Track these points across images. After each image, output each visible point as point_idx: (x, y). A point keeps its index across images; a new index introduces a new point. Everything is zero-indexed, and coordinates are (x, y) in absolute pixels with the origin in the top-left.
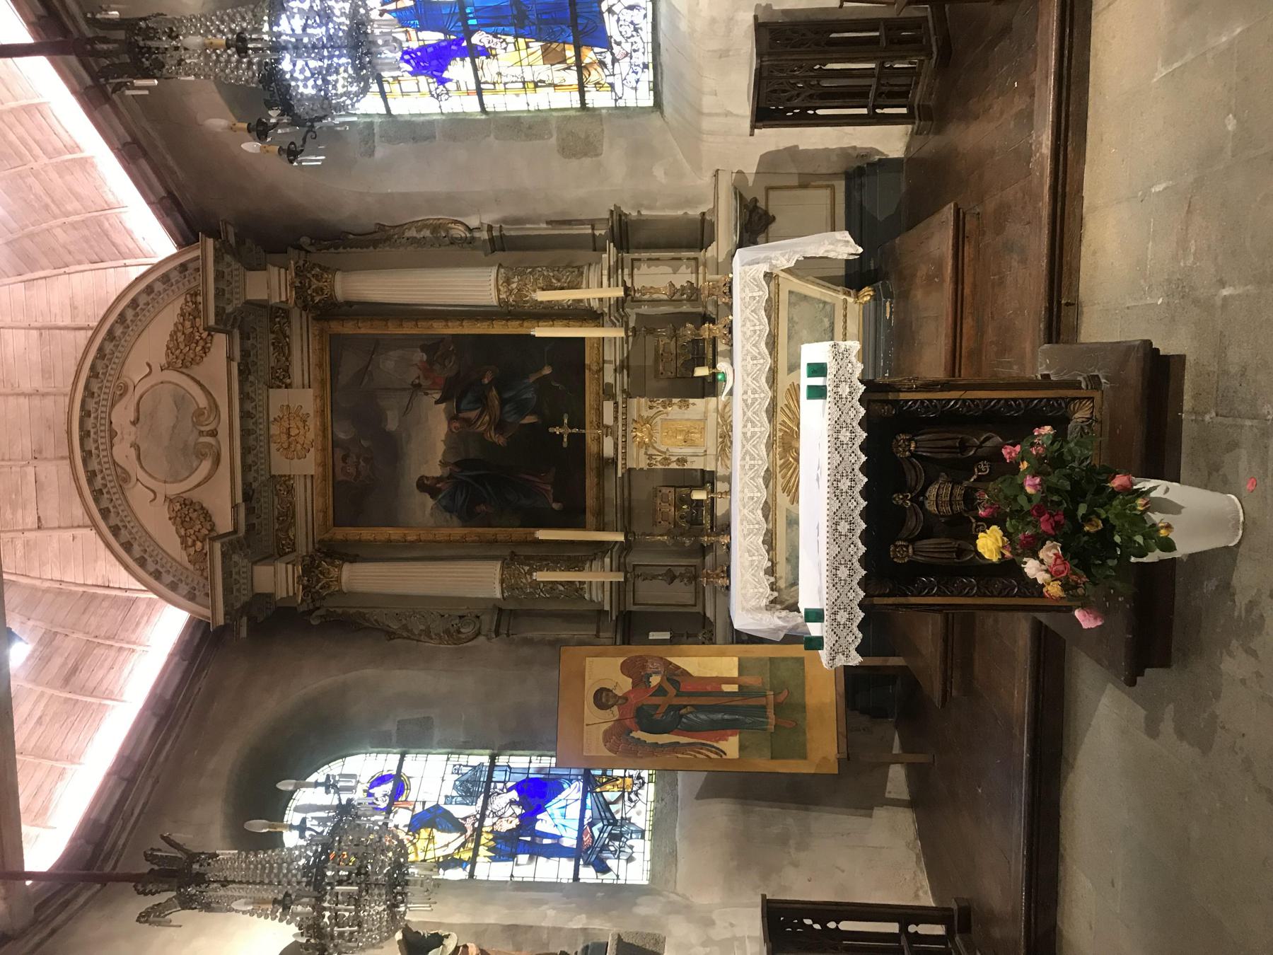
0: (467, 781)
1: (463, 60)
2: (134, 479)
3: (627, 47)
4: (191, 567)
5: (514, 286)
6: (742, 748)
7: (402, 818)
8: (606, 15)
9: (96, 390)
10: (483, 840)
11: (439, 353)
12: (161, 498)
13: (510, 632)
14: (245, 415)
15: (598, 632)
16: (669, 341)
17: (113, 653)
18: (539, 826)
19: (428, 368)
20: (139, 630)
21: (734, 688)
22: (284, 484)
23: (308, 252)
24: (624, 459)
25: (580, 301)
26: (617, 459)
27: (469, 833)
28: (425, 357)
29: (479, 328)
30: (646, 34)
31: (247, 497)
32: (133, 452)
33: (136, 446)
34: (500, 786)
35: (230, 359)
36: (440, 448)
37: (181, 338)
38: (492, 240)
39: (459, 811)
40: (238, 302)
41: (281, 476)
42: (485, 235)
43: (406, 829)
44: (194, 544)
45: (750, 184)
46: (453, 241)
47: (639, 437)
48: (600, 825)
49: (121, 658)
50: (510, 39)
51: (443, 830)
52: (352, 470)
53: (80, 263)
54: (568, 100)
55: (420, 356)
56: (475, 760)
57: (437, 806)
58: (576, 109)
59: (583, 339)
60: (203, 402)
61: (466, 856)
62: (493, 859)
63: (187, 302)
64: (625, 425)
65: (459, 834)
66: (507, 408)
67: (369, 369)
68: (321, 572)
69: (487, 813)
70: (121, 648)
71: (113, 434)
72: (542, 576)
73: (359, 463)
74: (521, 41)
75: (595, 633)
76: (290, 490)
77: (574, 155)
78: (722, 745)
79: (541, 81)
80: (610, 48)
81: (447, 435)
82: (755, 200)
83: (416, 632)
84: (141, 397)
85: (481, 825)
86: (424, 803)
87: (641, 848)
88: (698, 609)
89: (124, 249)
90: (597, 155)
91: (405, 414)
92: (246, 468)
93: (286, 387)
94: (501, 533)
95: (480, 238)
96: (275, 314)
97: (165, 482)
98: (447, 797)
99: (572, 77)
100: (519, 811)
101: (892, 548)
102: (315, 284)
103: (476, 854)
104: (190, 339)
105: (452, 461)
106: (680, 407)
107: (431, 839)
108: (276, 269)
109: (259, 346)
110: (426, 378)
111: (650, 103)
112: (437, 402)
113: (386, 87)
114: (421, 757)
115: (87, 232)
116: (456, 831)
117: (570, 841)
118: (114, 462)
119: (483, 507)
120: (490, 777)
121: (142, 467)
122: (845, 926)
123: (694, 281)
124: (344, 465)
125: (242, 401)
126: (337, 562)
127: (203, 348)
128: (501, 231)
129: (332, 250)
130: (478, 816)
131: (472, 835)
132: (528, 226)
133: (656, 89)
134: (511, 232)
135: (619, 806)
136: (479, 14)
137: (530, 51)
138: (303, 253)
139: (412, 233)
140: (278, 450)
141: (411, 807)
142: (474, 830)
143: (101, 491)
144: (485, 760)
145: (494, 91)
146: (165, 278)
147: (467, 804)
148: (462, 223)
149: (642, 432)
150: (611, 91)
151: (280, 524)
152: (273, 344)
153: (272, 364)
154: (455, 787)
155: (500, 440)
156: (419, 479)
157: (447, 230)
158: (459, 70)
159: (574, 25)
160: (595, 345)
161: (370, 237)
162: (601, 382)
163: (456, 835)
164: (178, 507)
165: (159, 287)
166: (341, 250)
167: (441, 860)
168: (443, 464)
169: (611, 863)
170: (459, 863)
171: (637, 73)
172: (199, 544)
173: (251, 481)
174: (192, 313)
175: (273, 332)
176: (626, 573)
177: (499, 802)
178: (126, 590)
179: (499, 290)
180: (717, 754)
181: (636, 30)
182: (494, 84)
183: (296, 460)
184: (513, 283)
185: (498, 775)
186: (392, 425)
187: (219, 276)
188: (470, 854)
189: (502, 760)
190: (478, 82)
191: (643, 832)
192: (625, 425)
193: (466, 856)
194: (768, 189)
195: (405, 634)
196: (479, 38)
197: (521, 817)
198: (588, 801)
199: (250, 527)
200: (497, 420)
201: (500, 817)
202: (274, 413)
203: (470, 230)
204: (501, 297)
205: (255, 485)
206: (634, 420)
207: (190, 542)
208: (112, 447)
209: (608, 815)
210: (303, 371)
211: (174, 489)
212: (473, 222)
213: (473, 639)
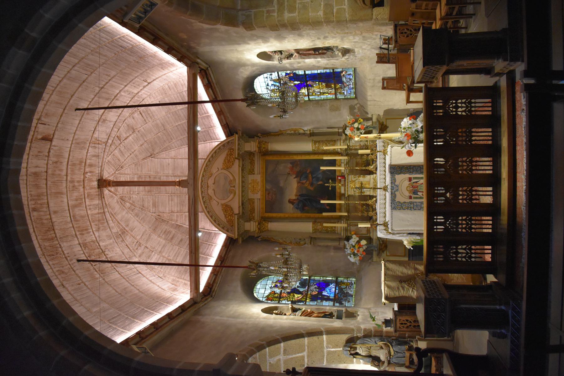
1: (305, 88)
2: (213, 199)
3: (348, 84)
4: (227, 223)
5: (317, 145)
8: (342, 77)
9: (205, 175)
10: (308, 296)
12: (220, 204)
14: (243, 182)
17: (207, 245)
19: (292, 169)
20: (213, 240)
22: (251, 201)
23: (260, 138)
24: (347, 192)
25: (335, 149)
28: (291, 166)
30: (353, 81)
31: (242, 204)
32: (213, 192)
33: (214, 190)
35: (239, 166)
37: (227, 161)
38: (310, 133)
39: (301, 290)
40: (243, 151)
41: (251, 199)
42: (308, 132)
44: (228, 217)
45: (382, 118)
46: (299, 134)
48: (340, 294)
49: (210, 247)
50: (317, 83)
53: (201, 142)
55: (290, 165)
58: (334, 99)
59: (335, 160)
60: (232, 178)
61: (303, 300)
63: (228, 151)
64: (348, 183)
66: (314, 179)
70: (209, 244)
71: (208, 187)
72: (325, 225)
74: (320, 83)
76: (253, 203)
81: (297, 187)
82: (383, 122)
83: (288, 243)
84: (216, 177)
85: (307, 293)
88: (368, 235)
89: (212, 138)
90: (340, 111)
91: (285, 181)
92: (242, 196)
94: (312, 215)
96: (251, 154)
97: (221, 200)
99: (333, 91)
102: (263, 146)
104: (229, 161)
105: (298, 195)
111: (354, 97)
112: (294, 178)
115: (204, 134)
118: (208, 194)
121: (215, 195)
125: (242, 178)
127: (232, 164)
133: (355, 93)
134: (315, 131)
135: (346, 289)
139: (289, 132)
143: (205, 202)
145: (312, 95)
146: (224, 145)
148: (302, 129)
153: (249, 168)
155: (311, 188)
157: (298, 131)
161: (277, 133)
163: (301, 295)
164: (224, 207)
165: (222, 147)
166: (269, 137)
168: (296, 195)
172: (229, 217)
174: (230, 154)
175: (250, 159)
176: (348, 224)
178: (209, 230)
179: (313, 147)
182: (312, 93)
185: (311, 281)
186: (282, 184)
187: (239, 144)
189: (313, 278)
192: (348, 183)
194: (386, 119)
195: (285, 243)
197: (318, 291)
198: (337, 288)
199: (243, 213)
201: (313, 291)
202: (250, 182)
203: (304, 131)
205: (244, 201)
207: (227, 216)
208: (208, 190)
211: (223, 202)
212: (306, 129)
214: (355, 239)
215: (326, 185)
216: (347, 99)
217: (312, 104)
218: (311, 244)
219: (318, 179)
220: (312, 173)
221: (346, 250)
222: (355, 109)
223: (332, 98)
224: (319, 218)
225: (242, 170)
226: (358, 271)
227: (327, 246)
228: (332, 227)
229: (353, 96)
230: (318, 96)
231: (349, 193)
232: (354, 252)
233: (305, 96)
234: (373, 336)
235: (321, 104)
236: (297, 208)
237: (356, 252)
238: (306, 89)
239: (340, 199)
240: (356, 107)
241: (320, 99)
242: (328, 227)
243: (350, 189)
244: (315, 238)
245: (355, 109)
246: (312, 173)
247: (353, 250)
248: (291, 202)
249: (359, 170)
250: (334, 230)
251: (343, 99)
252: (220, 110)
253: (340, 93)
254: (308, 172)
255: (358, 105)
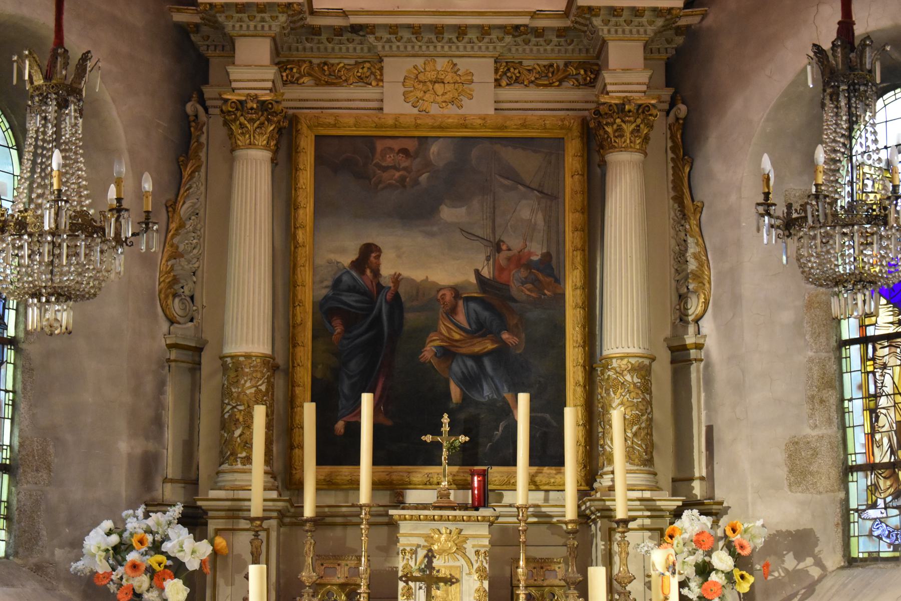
5: (628, 378)
11: (540, 276)
13: (173, 364)
14: (461, 31)
15: (172, 481)
16: (560, 577)
19: (521, 261)
23: (668, 113)
24: (412, 518)
25: (610, 461)
26: (403, 508)
28: (535, 258)
29: (574, 329)
31: (356, 29)
35: (534, 15)
36: (418, 275)
38: (684, 348)
40: (604, 32)
42: (690, 340)
46: (682, 298)
47: (439, 538)
52: (389, 160)
55: (537, 251)
58: (846, 459)
64: (455, 519)
66: (470, 363)
67: (520, 187)
68: (262, 124)
72: (260, 413)
73: (398, 170)
75: (170, 476)
76: (363, 81)
77: (790, 456)
79: (877, 417)
81: (434, 284)
83: (175, 241)
90: (790, 485)
92: (393, 29)
93: (496, 80)
94: (305, 355)
95: (687, 334)
102: (628, 128)
105: (402, 290)
106: (478, 590)
108: (647, 81)
109: (548, 48)
110: (509, 259)
111: (854, 554)
112: (477, 273)
119: (339, 329)
124: (397, 151)
125: (481, 27)
126: (273, 143)
128: (696, 360)
129: (670, 144)
132: (703, 395)
133: (874, 559)
134: (695, 372)
138: (666, 106)
139: (692, 249)
140: (415, 67)
145: (864, 359)
148: (705, 311)
149: (446, 541)
150: (867, 505)
151: (319, 65)
152: (551, 65)
153: (525, 63)
155: (429, 352)
156: (376, 246)
157: (695, 292)
160: (552, 480)
161: (686, 191)
162: (504, 487)
166: (670, 155)
168: (397, 279)
171: (888, 537)
173: (377, 35)
175: (566, 65)
179: (622, 358)
182: (873, 359)
183: (402, 89)
184: (632, 377)
186: (447, 213)
190: (875, 339)
192: (455, 519)
195: (173, 226)
199: (316, 31)
200: (453, 349)
202: (463, 64)
203: (697, 321)
204: (614, 361)
205: (371, 38)
206: (461, 530)
210: (517, 102)
212: (707, 325)
213: (166, 315)
214: (193, 552)
215: (446, 419)
216: (846, 523)
217: (824, 355)
218: (170, 347)
219: (470, 382)
220: (501, 355)
221: (140, 512)
222: (799, 557)
223: (850, 450)
224: (291, 384)
225: (517, 27)
226: (39, 569)
227: (158, 423)
228: (248, 445)
229: (860, 547)
230: (860, 387)
231: (405, 528)
232: (130, 548)
233: (863, 327)
235: (822, 401)
236: (337, 283)
237: (132, 557)
238: (892, 330)
239: (377, 485)
240: (809, 561)
241: (847, 396)
242: (248, 426)
243: (425, 528)
244: (195, 367)
245: (799, 557)
246: (501, 355)
247: (141, 542)
248: (369, 255)
249: (513, 575)
250: (234, 454)
251: (847, 499)
253: (873, 489)
254: (505, 336)
255: (815, 572)
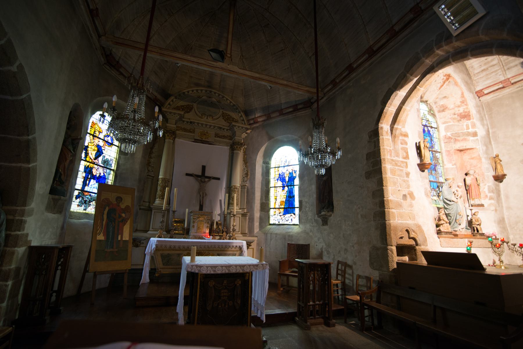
0: (108, 162)
4: (176, 106)
6: (100, 241)
7: (101, 143)
8: (290, 214)
10: (91, 164)
18: (92, 180)
21: (119, 239)
27: (94, 161)
30: (286, 223)
34: (105, 171)
39: (100, 159)
43: (98, 144)
48: (90, 198)
50: (286, 195)
51: (96, 154)
54: (272, 205)
56: (113, 165)
57: (103, 153)
61: (88, 159)
62: (85, 166)
65: (94, 158)
68: (172, 135)
69: (99, 167)
74: (286, 197)
78: (102, 234)
80: (283, 215)
85: (95, 164)
86: (104, 150)
87: (81, 210)
98: (105, 156)
99: (277, 206)
100: (98, 175)
101: (213, 281)
103: (88, 162)
107: (94, 150)
111: (271, 223)
113: (277, 168)
114: (116, 151)
116: (95, 158)
117: (87, 189)
120: (108, 169)
122: (59, 272)
123: (236, 231)
126: (173, 139)
129: (243, 152)
130: (98, 164)
131: (93, 161)
136: (291, 189)
137: (283, 198)
141: (104, 146)
142: (95, 162)
144: (113, 168)
145: (275, 190)
147: (102, 161)
154: (107, 159)
158: (280, 184)
159: (288, 208)
163: (94, 157)
166: (243, 154)
167: (88, 152)
169: (78, 200)
170: (86, 157)
177: (101, 170)
180: (99, 233)
181: (287, 221)
185: (108, 171)
188: (88, 160)
190: (277, 187)
191: (85, 210)
193: (88, 159)
194: (253, 249)
196: (286, 188)
201: (97, 170)
207: (182, 107)
209: (92, 200)
234: (8, 232)
252: (271, 117)
